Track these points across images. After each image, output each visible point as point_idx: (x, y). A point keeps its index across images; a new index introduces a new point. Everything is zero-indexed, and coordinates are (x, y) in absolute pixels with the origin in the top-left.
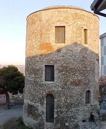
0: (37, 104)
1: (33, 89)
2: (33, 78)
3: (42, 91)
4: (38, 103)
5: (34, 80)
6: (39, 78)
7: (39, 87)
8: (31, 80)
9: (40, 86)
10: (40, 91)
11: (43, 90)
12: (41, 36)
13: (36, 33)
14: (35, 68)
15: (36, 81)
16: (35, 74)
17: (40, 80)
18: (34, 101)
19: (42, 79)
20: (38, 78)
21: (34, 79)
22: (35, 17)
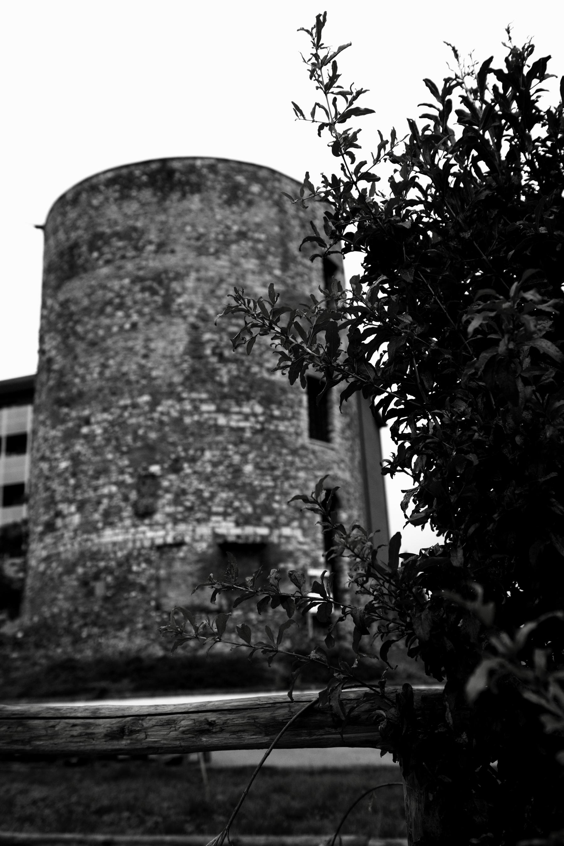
0: (286, 531)
1: (257, 466)
2: (252, 419)
3: (302, 474)
4: (287, 525)
5: (258, 426)
6: (289, 419)
7: (289, 458)
8: (242, 424)
9: (294, 452)
10: (293, 473)
11: (306, 469)
12: (284, 267)
13: (258, 241)
14: (266, 375)
15: (276, 432)
16: (266, 402)
17: (292, 430)
18: (268, 519)
19: (298, 426)
20: (282, 418)
21: (262, 423)
22: (247, 178)
